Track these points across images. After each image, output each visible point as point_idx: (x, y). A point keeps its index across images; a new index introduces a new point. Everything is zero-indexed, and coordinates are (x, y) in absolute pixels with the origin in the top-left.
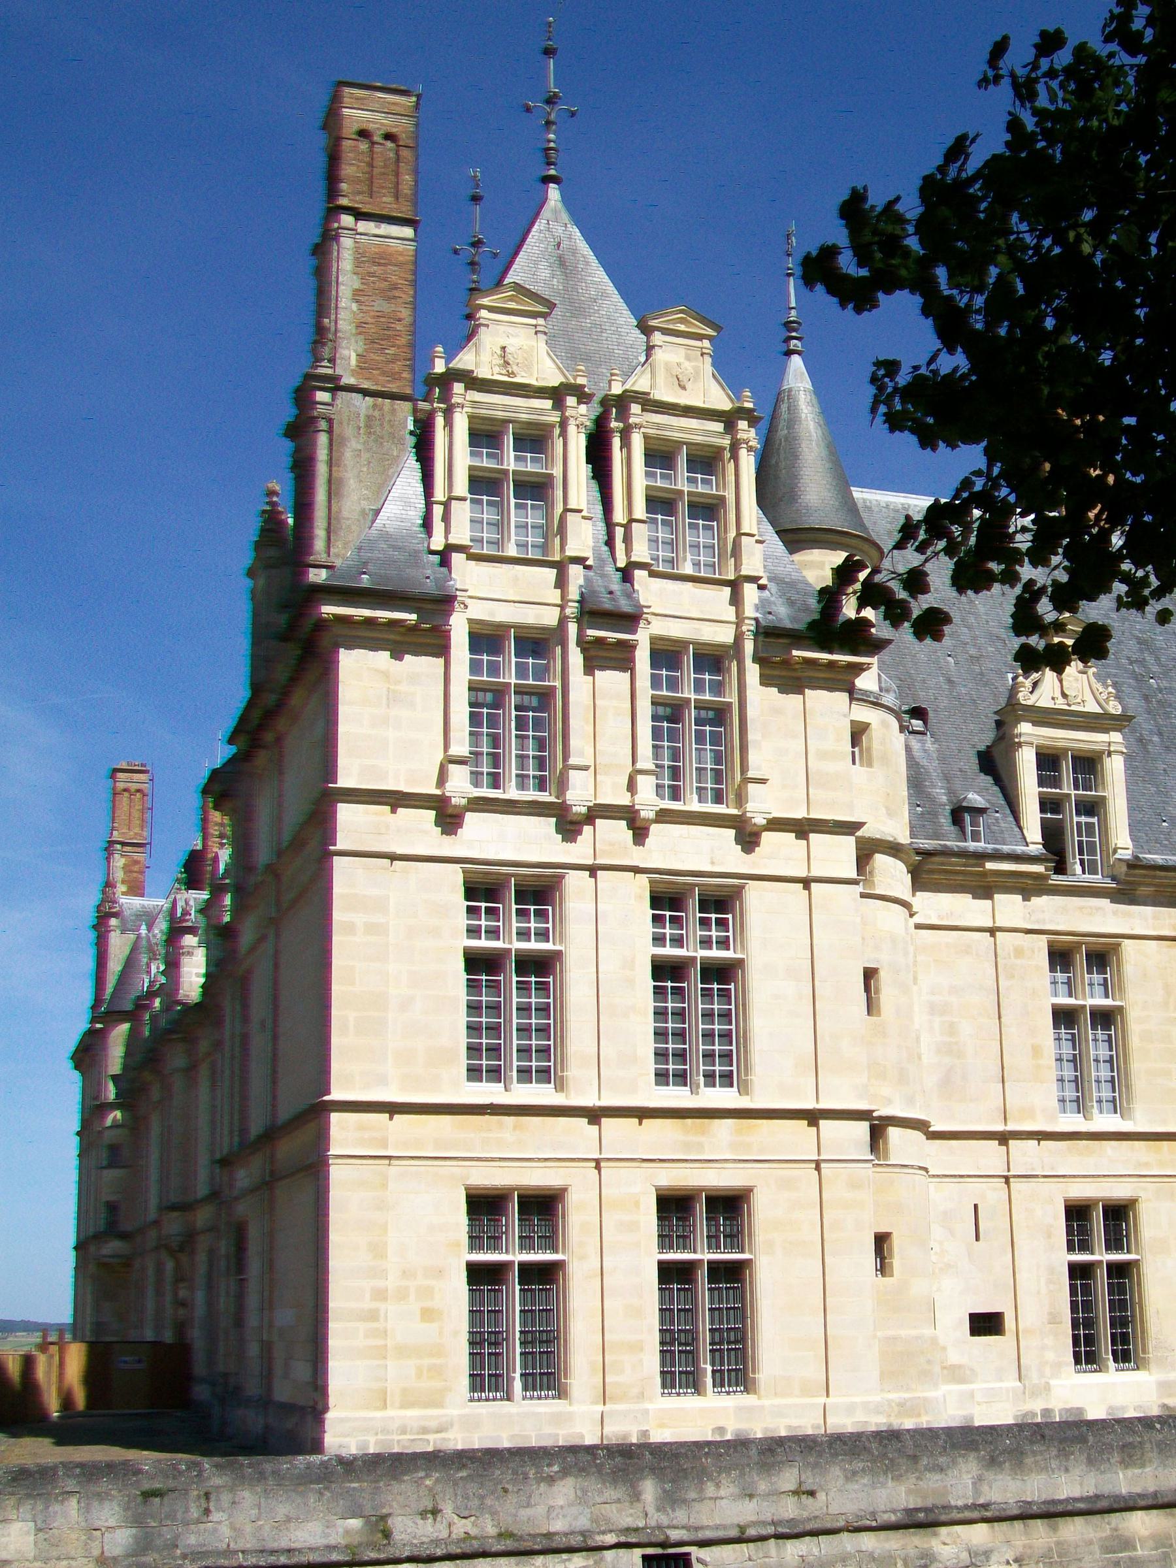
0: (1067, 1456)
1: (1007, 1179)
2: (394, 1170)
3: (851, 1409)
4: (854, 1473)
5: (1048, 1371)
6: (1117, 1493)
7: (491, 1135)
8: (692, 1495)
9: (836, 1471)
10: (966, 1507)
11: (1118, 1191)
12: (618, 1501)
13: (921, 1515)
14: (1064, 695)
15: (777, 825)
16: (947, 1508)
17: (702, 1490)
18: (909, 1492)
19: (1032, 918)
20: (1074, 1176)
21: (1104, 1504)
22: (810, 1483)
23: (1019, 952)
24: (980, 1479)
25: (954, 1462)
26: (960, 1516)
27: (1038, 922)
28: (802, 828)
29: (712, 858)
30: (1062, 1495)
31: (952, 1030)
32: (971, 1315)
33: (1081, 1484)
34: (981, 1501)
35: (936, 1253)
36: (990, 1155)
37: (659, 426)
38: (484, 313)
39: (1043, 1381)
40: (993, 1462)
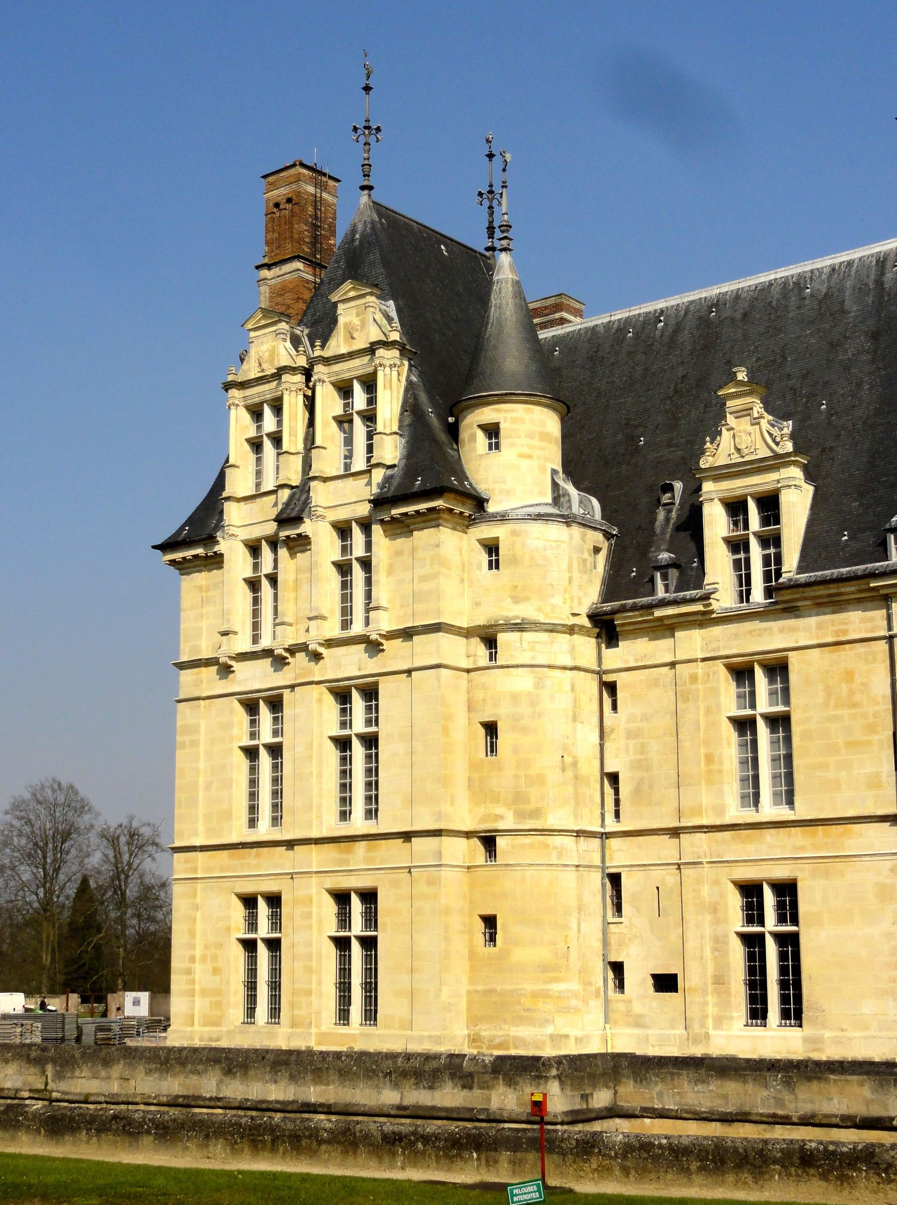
0: (276, 1072)
1: (679, 866)
2: (199, 886)
3: (420, 1039)
4: (151, 1071)
5: (710, 1022)
6: (309, 1101)
7: (245, 861)
8: (69, 1075)
9: (141, 1068)
10: (211, 1099)
11: (781, 873)
12: (35, 1074)
13: (181, 1100)
14: (738, 450)
15: (391, 635)
16: (199, 1097)
17: (73, 1073)
18: (180, 1085)
19: (709, 648)
20: (736, 861)
21: (264, 1106)
22: (126, 1074)
23: (694, 678)
24: (221, 1081)
25: (206, 1071)
26: (207, 1103)
27: (714, 650)
28: (407, 634)
29: (360, 666)
30: (272, 1097)
31: (643, 749)
33: (285, 1092)
34: (221, 1096)
35: (626, 927)
36: (665, 848)
37: (337, 373)
38: (252, 334)
39: (704, 1030)
40: (229, 1072)
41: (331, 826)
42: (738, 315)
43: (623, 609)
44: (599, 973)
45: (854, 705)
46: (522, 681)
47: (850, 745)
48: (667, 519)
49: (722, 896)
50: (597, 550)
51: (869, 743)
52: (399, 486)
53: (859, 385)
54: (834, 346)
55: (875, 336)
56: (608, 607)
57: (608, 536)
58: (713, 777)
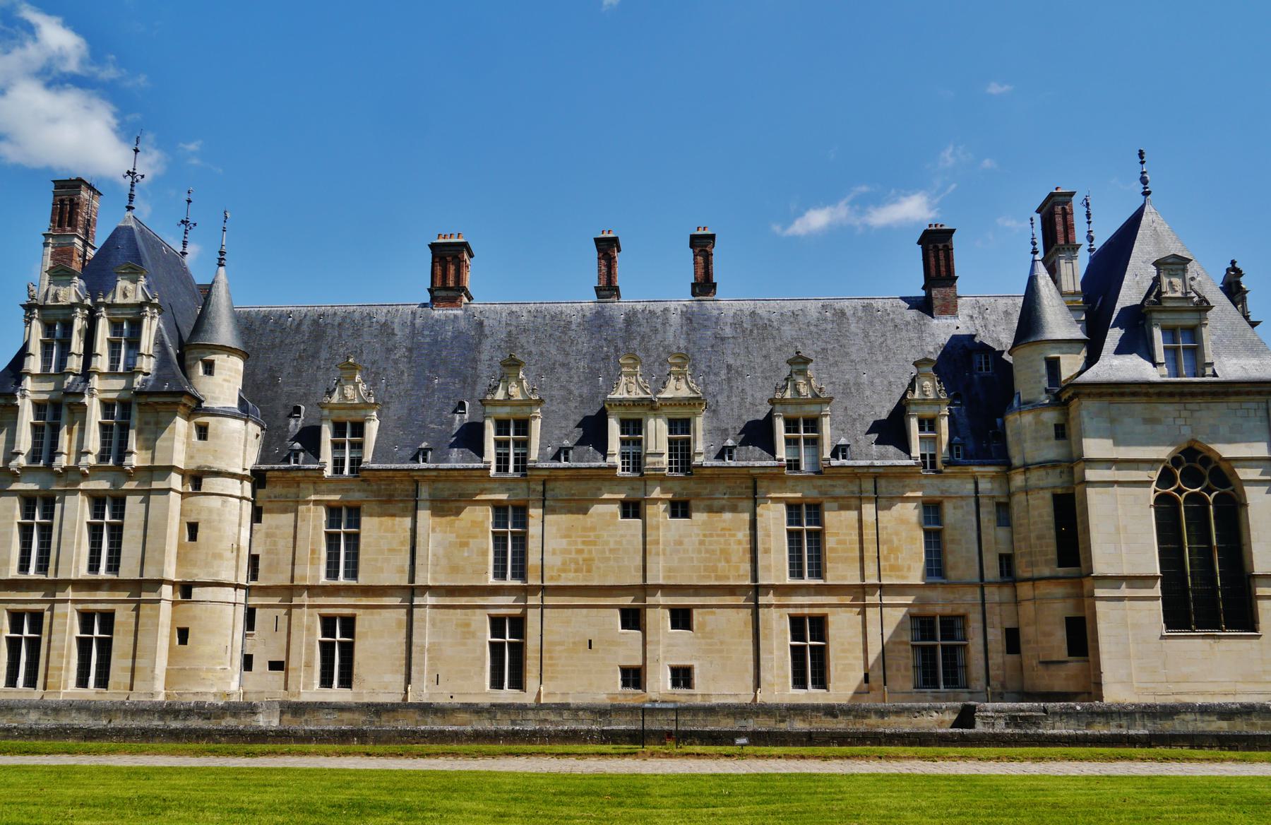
31: (275, 544)
32: (269, 662)
41: (83, 572)
42: (336, 323)
43: (273, 470)
44: (238, 661)
45: (394, 532)
46: (215, 502)
47: (390, 550)
48: (296, 425)
49: (314, 622)
50: (257, 436)
51: (400, 550)
52: (153, 385)
53: (402, 372)
54: (389, 350)
55: (410, 350)
56: (263, 467)
57: (263, 429)
58: (314, 561)
